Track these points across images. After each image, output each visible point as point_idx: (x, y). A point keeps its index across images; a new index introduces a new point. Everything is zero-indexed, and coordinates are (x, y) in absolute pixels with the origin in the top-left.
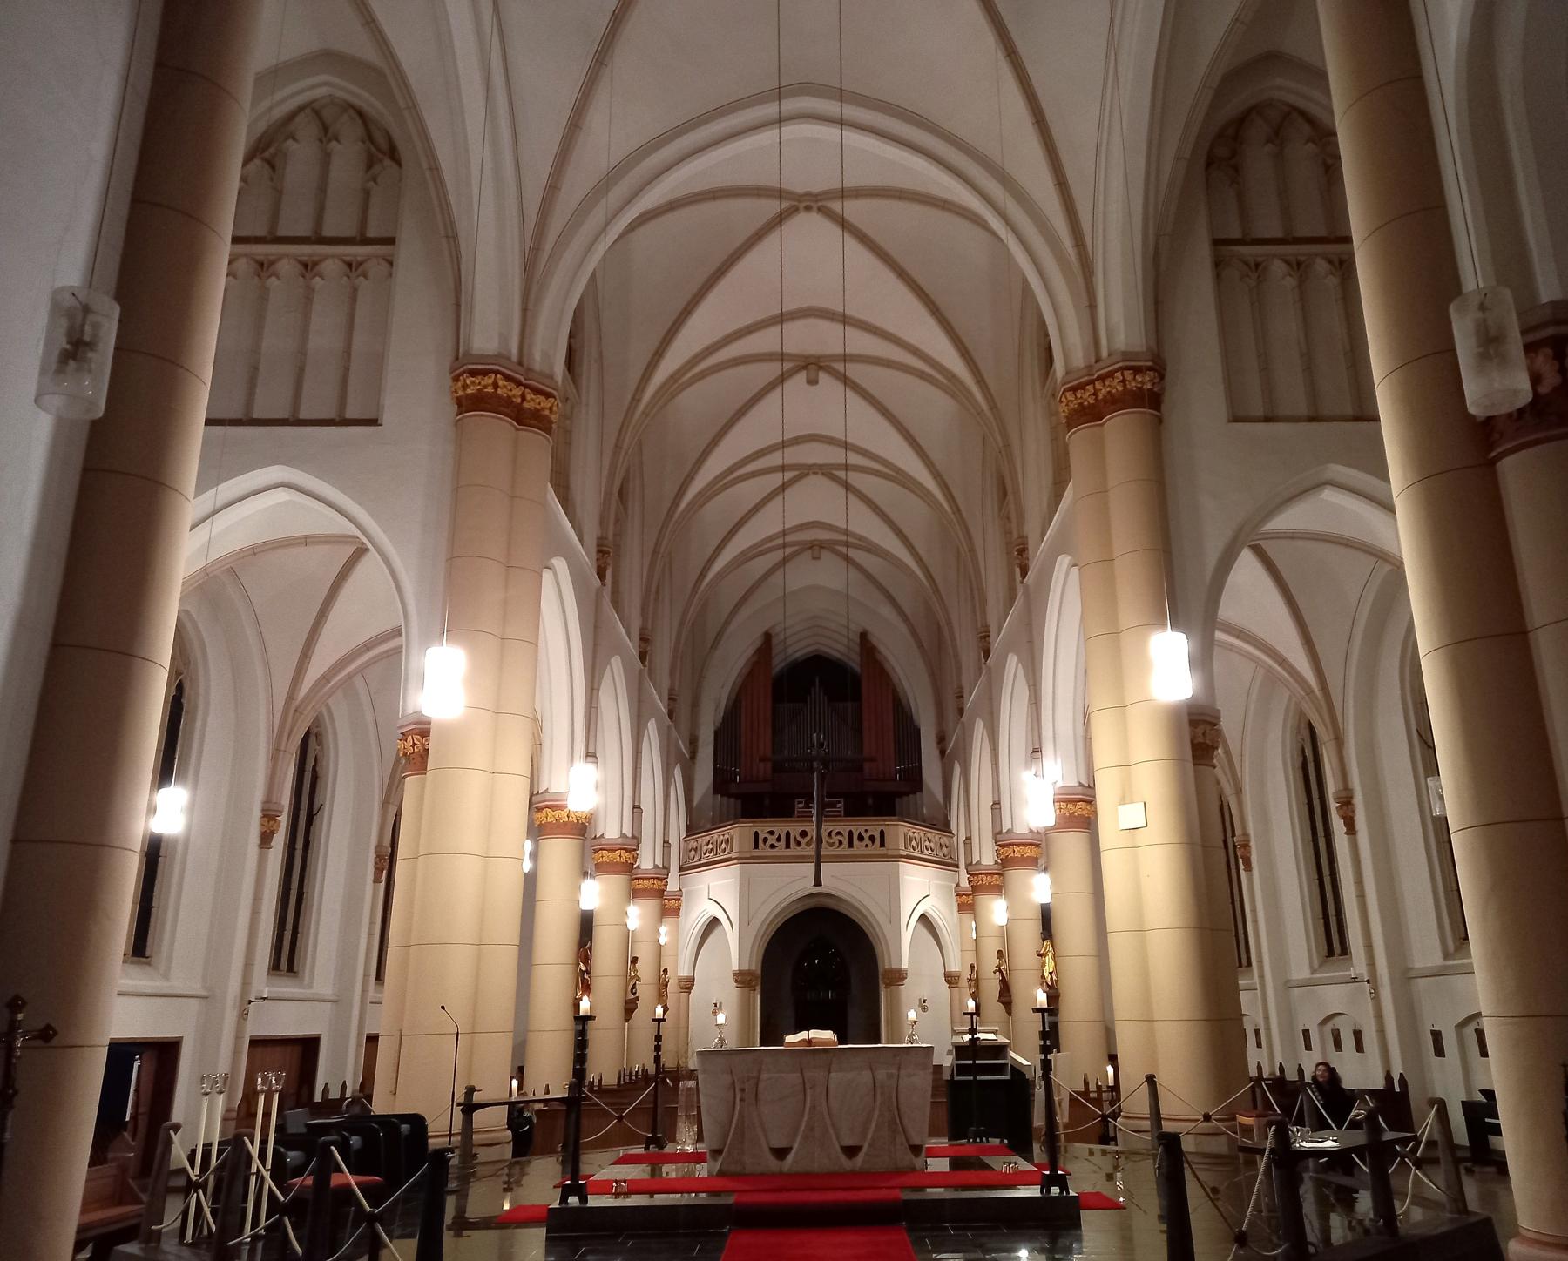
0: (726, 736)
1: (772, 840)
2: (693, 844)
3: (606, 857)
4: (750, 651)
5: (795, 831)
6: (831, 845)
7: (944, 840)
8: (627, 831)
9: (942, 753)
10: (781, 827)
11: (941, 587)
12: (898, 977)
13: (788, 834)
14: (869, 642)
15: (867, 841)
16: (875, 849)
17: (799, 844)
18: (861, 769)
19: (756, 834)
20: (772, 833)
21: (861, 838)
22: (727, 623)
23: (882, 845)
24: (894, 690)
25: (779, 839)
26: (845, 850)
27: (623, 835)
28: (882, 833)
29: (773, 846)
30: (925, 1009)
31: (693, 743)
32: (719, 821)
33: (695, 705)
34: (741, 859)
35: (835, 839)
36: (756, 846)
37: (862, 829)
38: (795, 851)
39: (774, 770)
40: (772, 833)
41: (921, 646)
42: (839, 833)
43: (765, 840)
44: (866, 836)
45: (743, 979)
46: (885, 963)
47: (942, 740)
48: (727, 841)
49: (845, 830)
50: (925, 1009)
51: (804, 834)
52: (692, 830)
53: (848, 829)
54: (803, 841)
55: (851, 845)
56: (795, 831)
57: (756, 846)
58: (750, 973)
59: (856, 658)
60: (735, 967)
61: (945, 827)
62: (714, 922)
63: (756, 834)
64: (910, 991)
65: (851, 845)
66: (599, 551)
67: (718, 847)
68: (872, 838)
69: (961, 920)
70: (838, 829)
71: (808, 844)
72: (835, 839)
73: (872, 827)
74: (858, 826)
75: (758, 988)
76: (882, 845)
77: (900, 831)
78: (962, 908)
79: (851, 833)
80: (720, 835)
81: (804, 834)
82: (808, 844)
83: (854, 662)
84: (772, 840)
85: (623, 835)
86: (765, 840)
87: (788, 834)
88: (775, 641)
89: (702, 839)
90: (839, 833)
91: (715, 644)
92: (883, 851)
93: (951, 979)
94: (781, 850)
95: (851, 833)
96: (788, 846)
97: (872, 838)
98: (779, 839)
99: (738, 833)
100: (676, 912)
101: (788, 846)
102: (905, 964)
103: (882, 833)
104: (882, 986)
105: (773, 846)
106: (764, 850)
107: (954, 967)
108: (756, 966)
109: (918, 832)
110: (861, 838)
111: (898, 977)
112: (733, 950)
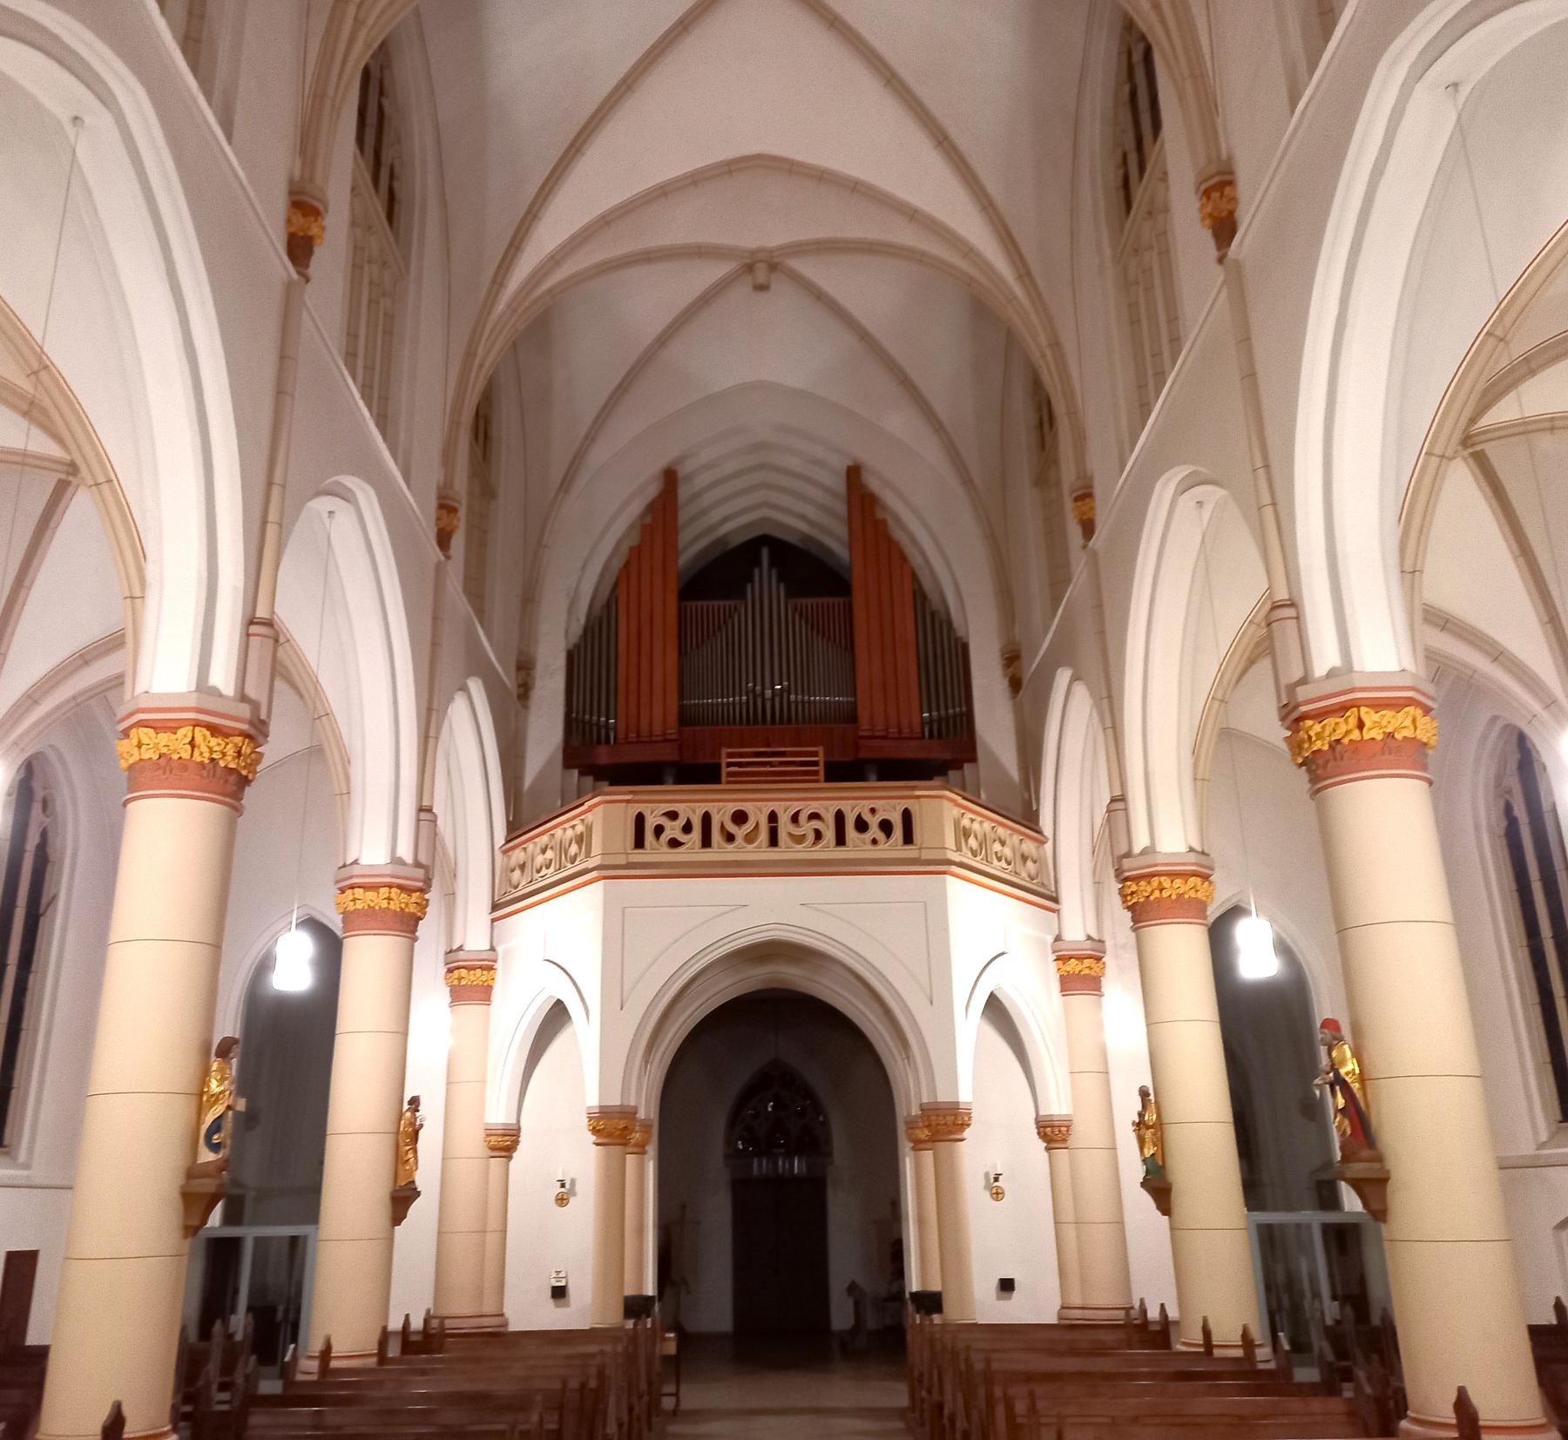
0: (588, 664)
1: (673, 830)
2: (518, 856)
3: (367, 899)
4: (636, 508)
5: (721, 813)
6: (799, 839)
7: (1029, 847)
8: (405, 851)
9: (1015, 685)
10: (692, 803)
11: (1036, 269)
12: (946, 1123)
13: (706, 819)
14: (862, 486)
15: (874, 831)
16: (893, 847)
17: (730, 838)
18: (852, 718)
19: (640, 820)
20: (673, 816)
21: (861, 826)
22: (590, 438)
23: (908, 838)
24: (919, 596)
25: (687, 828)
26: (827, 850)
27: (397, 861)
28: (907, 816)
29: (674, 843)
30: (998, 1195)
31: (525, 668)
32: (569, 802)
33: (529, 600)
34: (610, 871)
35: (807, 827)
36: (639, 843)
37: (863, 807)
38: (721, 851)
39: (684, 718)
40: (673, 816)
41: (967, 482)
42: (814, 816)
43: (659, 830)
44: (873, 822)
45: (611, 1127)
46: (911, 1098)
47: (1012, 659)
48: (579, 839)
49: (828, 809)
50: (998, 1195)
51: (740, 818)
52: (517, 827)
53: (834, 806)
54: (740, 832)
55: (841, 840)
56: (721, 813)
57: (639, 843)
58: (627, 1113)
59: (841, 530)
60: (593, 1100)
61: (1028, 818)
62: (557, 1016)
63: (640, 820)
64: (976, 1154)
65: (841, 840)
66: (441, 507)
67: (563, 849)
68: (886, 827)
69: (1067, 1009)
70: (814, 806)
71: (750, 838)
72: (807, 827)
73: (885, 801)
74: (855, 801)
75: (652, 1150)
76: (908, 838)
77: (944, 812)
78: (1068, 984)
79: (840, 817)
80: (565, 830)
81: (740, 818)
82: (750, 838)
83: (835, 539)
84: (673, 830)
85: (397, 861)
86: (659, 830)
87: (706, 819)
88: (683, 493)
89: (535, 847)
90: (814, 816)
91: (567, 482)
92: (909, 852)
93: (1052, 1133)
94: (692, 849)
95: (840, 817)
96: (706, 842)
97: (886, 827)
98: (687, 828)
99: (603, 817)
100: (484, 994)
101: (706, 842)
102: (965, 1096)
103: (907, 816)
104: (905, 1147)
105: (674, 843)
106: (656, 851)
107: (1057, 1105)
108: (647, 1110)
109: (981, 824)
110: (861, 826)
111: (946, 1123)
112: (592, 1069)
